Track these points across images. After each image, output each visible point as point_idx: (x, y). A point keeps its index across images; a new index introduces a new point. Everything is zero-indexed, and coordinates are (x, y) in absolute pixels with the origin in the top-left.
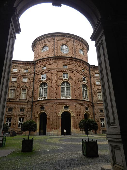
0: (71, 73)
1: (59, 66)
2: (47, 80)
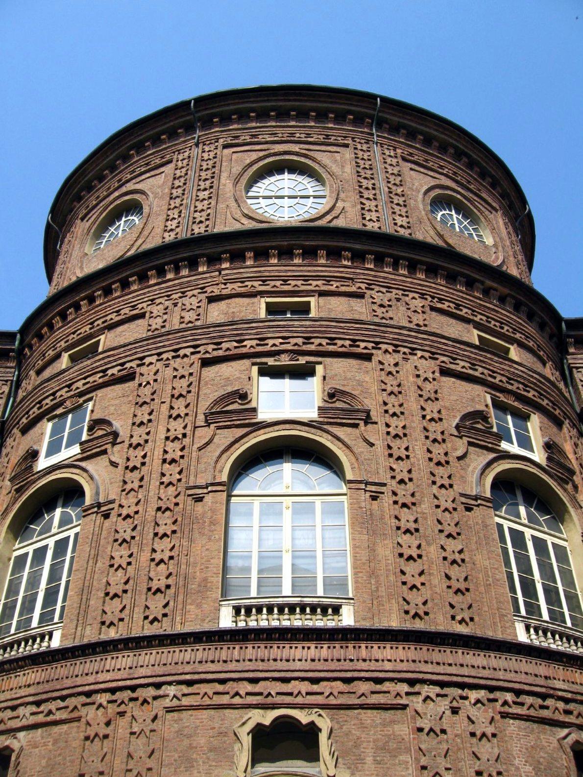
2: (90, 452)
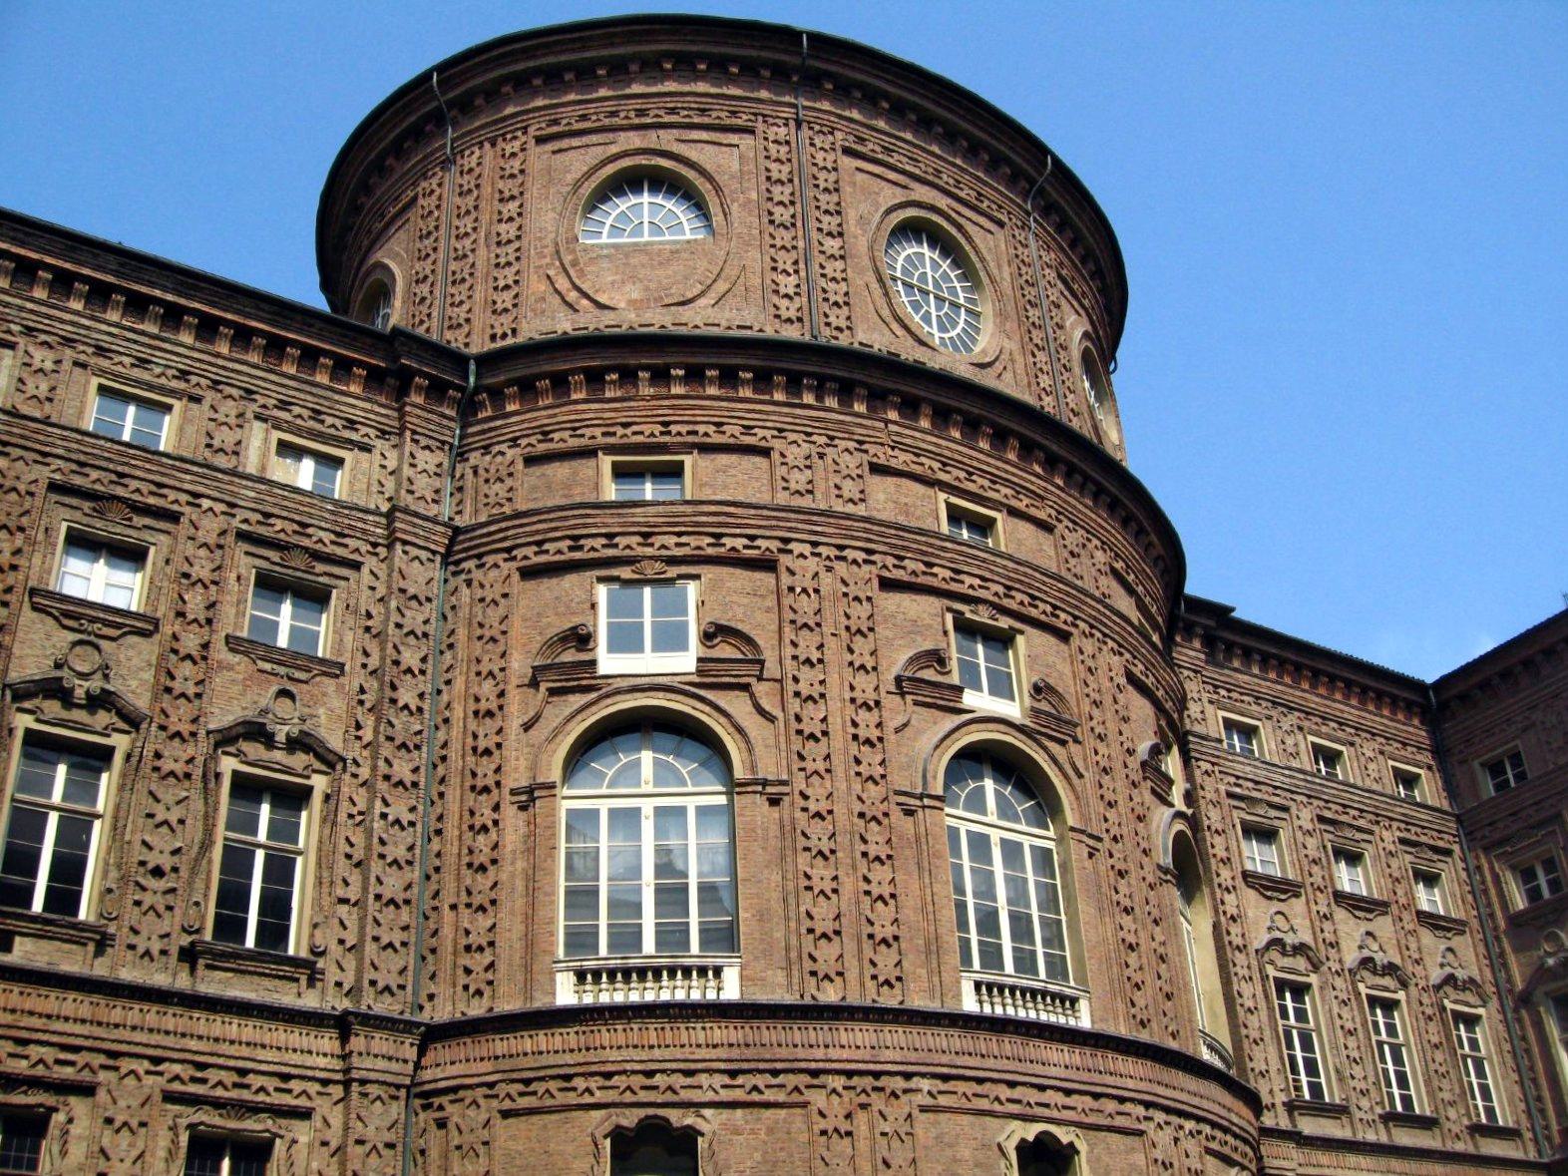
1: (886, 499)
2: (710, 677)
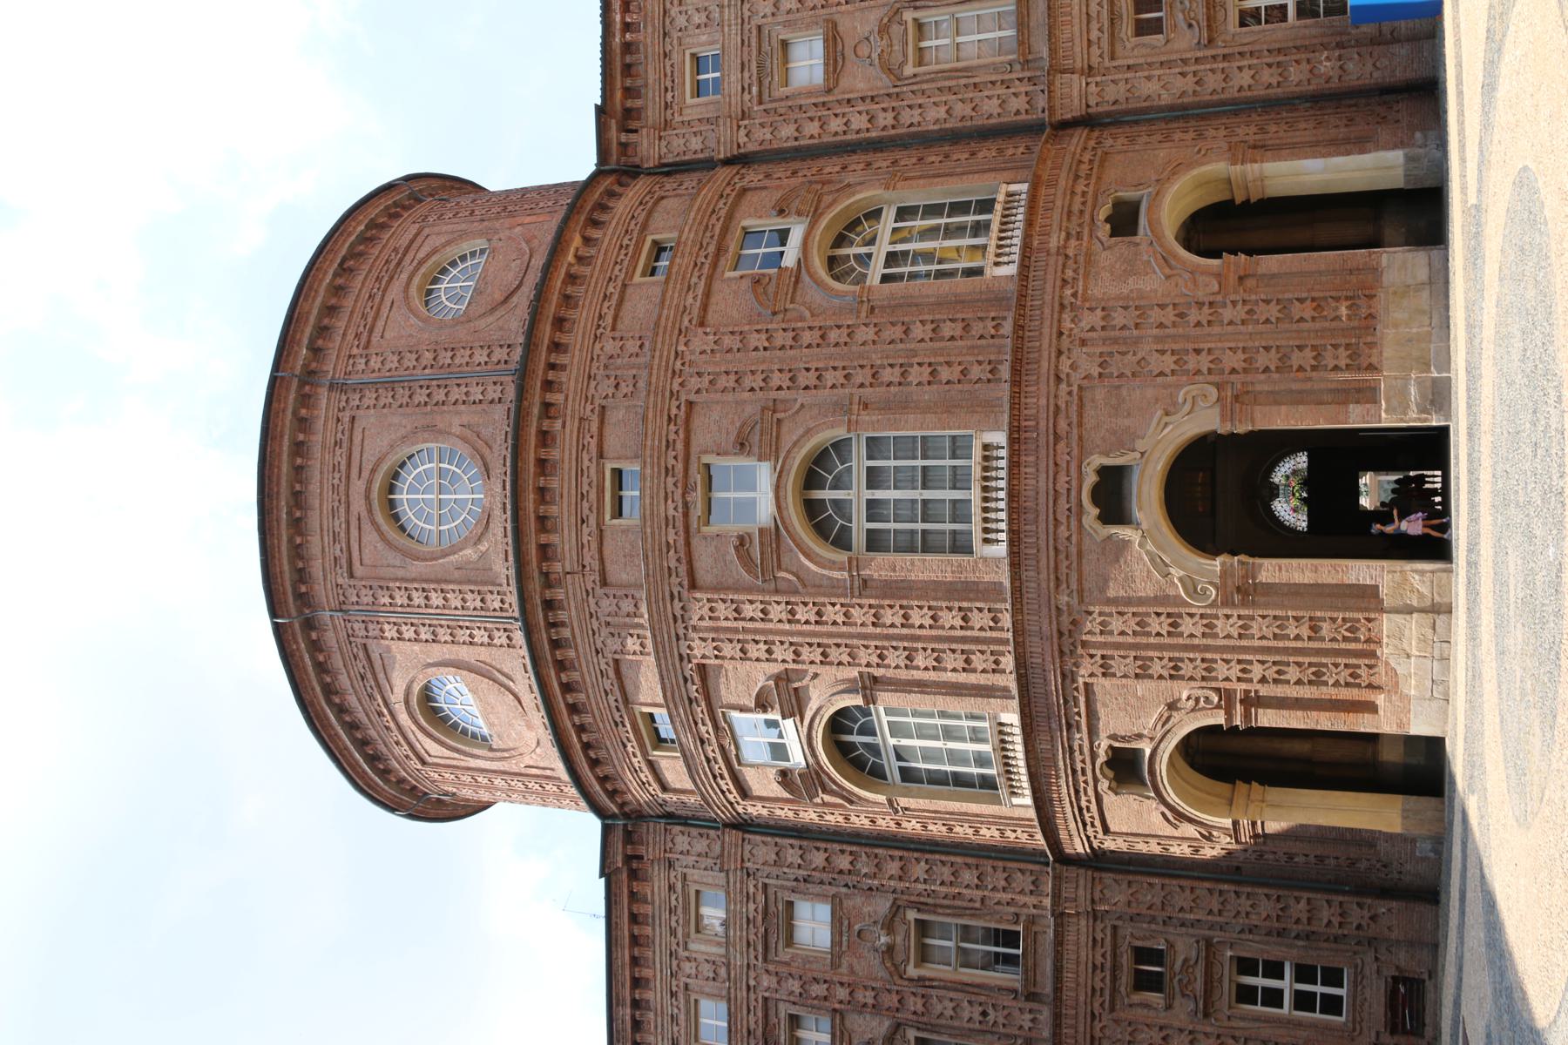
0: (697, 422)
2: (794, 705)
